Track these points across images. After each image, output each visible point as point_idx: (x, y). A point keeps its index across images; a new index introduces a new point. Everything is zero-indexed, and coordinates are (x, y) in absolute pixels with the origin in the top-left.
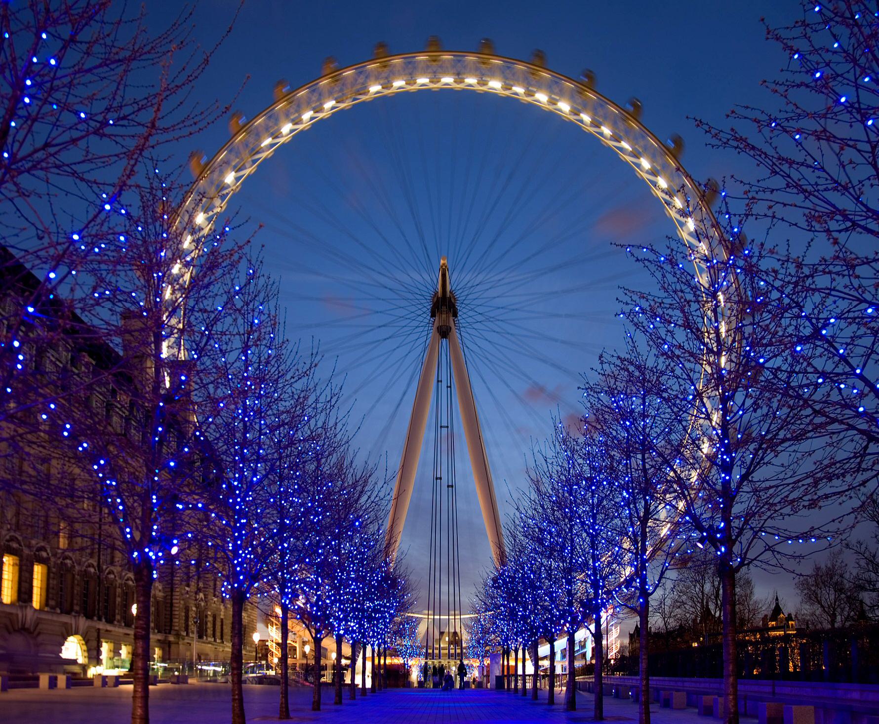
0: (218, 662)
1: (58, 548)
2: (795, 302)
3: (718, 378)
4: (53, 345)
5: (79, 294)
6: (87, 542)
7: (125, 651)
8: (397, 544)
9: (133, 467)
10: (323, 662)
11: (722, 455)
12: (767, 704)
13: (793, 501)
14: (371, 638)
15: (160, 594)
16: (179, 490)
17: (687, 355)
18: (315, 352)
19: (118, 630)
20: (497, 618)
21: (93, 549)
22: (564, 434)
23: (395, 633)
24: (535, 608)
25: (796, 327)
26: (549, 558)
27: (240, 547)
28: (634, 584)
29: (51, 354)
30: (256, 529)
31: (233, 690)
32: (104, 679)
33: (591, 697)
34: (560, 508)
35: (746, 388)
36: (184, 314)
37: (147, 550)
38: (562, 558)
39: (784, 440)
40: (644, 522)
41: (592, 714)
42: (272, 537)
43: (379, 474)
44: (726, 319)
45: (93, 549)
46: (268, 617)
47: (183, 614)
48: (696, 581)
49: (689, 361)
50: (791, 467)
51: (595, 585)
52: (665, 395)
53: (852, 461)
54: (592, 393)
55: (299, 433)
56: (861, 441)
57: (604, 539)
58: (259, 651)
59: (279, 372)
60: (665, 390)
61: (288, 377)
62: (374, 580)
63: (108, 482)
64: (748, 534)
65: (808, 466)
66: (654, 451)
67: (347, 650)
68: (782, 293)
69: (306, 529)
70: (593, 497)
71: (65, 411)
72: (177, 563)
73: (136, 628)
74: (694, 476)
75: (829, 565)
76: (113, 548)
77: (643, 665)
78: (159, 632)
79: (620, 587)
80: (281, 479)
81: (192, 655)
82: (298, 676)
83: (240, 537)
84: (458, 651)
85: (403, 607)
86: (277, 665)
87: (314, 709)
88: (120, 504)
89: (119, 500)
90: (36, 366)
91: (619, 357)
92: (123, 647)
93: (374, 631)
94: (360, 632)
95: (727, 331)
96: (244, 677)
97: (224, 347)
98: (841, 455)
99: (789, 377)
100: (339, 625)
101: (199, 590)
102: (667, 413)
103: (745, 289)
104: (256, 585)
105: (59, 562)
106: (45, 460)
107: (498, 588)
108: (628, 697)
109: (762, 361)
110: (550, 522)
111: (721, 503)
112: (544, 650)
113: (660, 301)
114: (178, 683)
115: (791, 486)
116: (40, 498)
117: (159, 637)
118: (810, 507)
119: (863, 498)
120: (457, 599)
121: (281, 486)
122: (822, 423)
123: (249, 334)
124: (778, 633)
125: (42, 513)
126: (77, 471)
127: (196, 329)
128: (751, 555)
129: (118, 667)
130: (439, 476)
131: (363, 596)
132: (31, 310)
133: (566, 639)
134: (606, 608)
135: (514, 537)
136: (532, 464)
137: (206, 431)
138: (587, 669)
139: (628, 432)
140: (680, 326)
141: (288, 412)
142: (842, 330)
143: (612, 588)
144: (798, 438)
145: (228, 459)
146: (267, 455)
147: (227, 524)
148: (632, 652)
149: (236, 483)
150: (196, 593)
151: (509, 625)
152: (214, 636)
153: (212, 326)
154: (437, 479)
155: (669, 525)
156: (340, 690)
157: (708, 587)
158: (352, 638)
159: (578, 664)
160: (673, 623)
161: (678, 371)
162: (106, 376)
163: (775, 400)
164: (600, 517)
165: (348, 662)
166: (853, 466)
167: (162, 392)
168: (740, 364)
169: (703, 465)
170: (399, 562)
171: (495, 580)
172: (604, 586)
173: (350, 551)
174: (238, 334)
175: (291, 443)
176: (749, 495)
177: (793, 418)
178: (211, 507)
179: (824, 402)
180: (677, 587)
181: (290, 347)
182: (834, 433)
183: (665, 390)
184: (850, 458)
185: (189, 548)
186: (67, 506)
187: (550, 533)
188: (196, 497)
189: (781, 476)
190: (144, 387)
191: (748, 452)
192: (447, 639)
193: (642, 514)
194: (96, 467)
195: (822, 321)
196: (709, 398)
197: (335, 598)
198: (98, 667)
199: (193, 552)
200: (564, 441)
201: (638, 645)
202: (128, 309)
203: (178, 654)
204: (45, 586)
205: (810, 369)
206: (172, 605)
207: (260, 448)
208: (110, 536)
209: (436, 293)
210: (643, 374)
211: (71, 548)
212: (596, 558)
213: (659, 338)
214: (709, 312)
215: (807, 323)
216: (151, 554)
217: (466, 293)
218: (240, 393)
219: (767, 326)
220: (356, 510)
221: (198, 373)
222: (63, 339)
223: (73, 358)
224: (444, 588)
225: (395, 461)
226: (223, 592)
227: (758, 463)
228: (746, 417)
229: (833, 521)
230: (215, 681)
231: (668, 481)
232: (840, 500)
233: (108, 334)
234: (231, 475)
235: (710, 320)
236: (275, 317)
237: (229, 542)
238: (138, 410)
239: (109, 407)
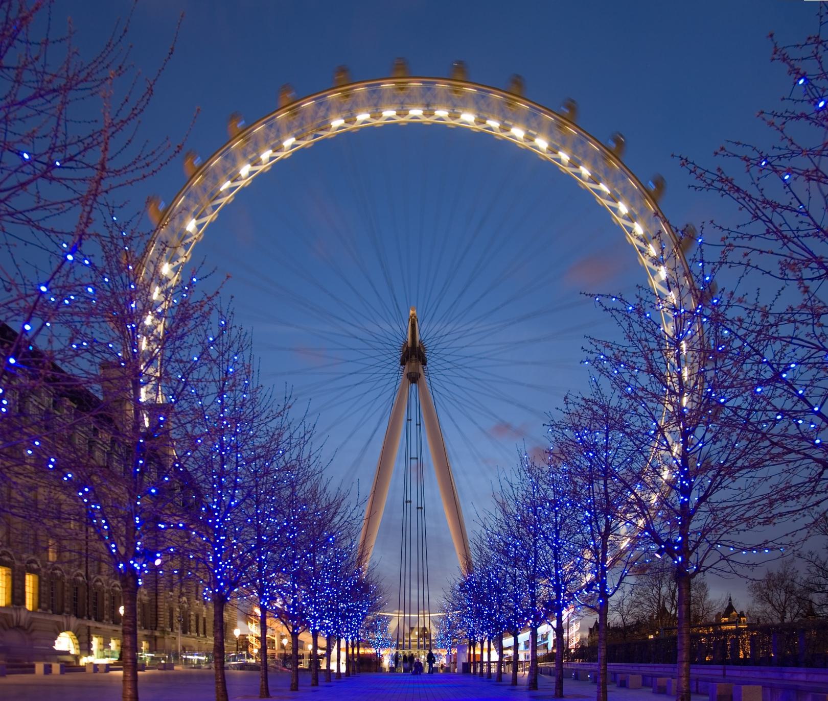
0: (200, 652)
1: (48, 561)
2: (755, 350)
3: (680, 415)
4: (33, 391)
5: (57, 346)
6: (74, 556)
7: (114, 645)
8: (369, 556)
9: (117, 494)
10: (300, 652)
11: (682, 480)
12: (718, 685)
13: (749, 518)
14: (345, 632)
15: (145, 599)
16: (161, 513)
17: (650, 396)
18: (288, 396)
19: (108, 627)
20: (464, 616)
21: (81, 562)
22: (530, 464)
23: (367, 628)
24: (500, 608)
25: (757, 371)
26: (514, 566)
27: (220, 559)
28: (594, 588)
29: (33, 399)
30: (234, 544)
31: (216, 675)
32: (96, 667)
33: (553, 679)
34: (525, 525)
35: (707, 424)
36: (161, 364)
37: (132, 562)
38: (526, 566)
39: (741, 468)
40: (605, 537)
41: (553, 693)
42: (250, 551)
43: (351, 500)
44: (689, 365)
45: (81, 562)
46: (247, 617)
47: (168, 614)
48: (653, 585)
49: (652, 401)
50: (748, 491)
51: (557, 589)
52: (628, 430)
53: (806, 485)
54: (557, 429)
55: (275, 464)
56: (816, 468)
57: (566, 551)
58: (239, 643)
59: (254, 413)
60: (628, 426)
61: (263, 417)
62: (347, 586)
63: (93, 506)
64: (704, 546)
65: (764, 489)
66: (616, 477)
67: (322, 642)
68: (744, 341)
69: (282, 544)
70: (556, 516)
71: (49, 447)
72: (161, 572)
73: (124, 625)
74: (654, 498)
75: (781, 572)
76: (100, 560)
77: (602, 653)
78: (145, 628)
79: (581, 590)
80: (258, 503)
81: (177, 647)
82: (277, 664)
83: (220, 551)
84: (427, 643)
85: (375, 607)
86: (257, 655)
87: (292, 690)
88: (105, 524)
89: (103, 521)
90: (20, 410)
91: (583, 399)
92: (112, 641)
93: (347, 627)
94: (334, 628)
95: (689, 376)
96: (226, 664)
97: (200, 392)
98: (796, 480)
99: (748, 415)
100: (315, 623)
101: (182, 595)
102: (629, 445)
103: (709, 338)
104: (236, 590)
105: (49, 572)
106: (32, 488)
107: (466, 591)
108: (587, 679)
109: (722, 400)
110: (515, 537)
111: (680, 521)
112: (508, 641)
113: (624, 349)
114: (164, 669)
115: (747, 506)
116: (29, 519)
117: (146, 632)
118: (764, 523)
119: (816, 516)
120: (426, 600)
121: (257, 509)
122: (779, 453)
123: (224, 381)
124: (730, 627)
125: (32, 532)
126: (63, 497)
127: (173, 377)
128: (706, 564)
129: (108, 657)
130: (409, 499)
131: (337, 599)
132: (12, 361)
133: (529, 632)
134: (567, 607)
135: (481, 550)
136: (497, 488)
137: (184, 463)
138: (549, 657)
139: (591, 462)
140: (643, 371)
141: (263, 447)
142: (802, 374)
143: (573, 591)
144: (755, 466)
145: (207, 486)
146: (244, 483)
147: (207, 540)
148: (592, 643)
149: (214, 507)
150: (179, 597)
151: (475, 622)
152: (197, 631)
153: (188, 374)
154: (407, 502)
155: (629, 539)
156: (317, 674)
157: (664, 590)
158: (327, 633)
159: (540, 653)
160: (630, 620)
161: (641, 410)
162: (87, 417)
163: (734, 434)
164: (563, 533)
165: (324, 652)
166: (807, 489)
167: (142, 431)
168: (701, 404)
169: (663, 489)
170: (371, 570)
171: (462, 586)
172: (566, 590)
173: (325, 562)
174: (214, 380)
175: (267, 473)
176: (706, 514)
177: (751, 449)
178: (192, 526)
179: (781, 436)
180: (635, 590)
181: (264, 392)
182: (790, 462)
183: (628, 426)
184: (805, 483)
185: (172, 560)
186: (55, 526)
187: (515, 546)
188: (177, 518)
189: (738, 498)
190: (125, 426)
191: (707, 478)
192: (417, 633)
193: (603, 530)
194: (80, 494)
195: (783, 366)
196: (670, 432)
197: (311, 600)
198: (89, 657)
199: (176, 563)
200: (529, 470)
201: (597, 637)
202: (107, 360)
203: (164, 646)
204: (36, 591)
205: (769, 408)
206: (157, 607)
207: (237, 477)
208: (96, 551)
209: (406, 343)
210: (607, 412)
211: (60, 560)
212: (558, 567)
213: (623, 382)
214: (672, 360)
215: (768, 368)
216: (136, 565)
217: (435, 343)
218: (217, 431)
219: (729, 371)
220: (330, 528)
221: (176, 414)
222: (45, 386)
223: (55, 402)
224: (414, 592)
225: (367, 487)
226: (205, 596)
227: (716, 487)
228: (706, 449)
229: (787, 535)
230: (200, 668)
231: (628, 503)
232: (794, 518)
233: (88, 382)
234: (210, 500)
235: (674, 366)
236: (249, 366)
237: (209, 556)
238: (119, 446)
239: (91, 444)
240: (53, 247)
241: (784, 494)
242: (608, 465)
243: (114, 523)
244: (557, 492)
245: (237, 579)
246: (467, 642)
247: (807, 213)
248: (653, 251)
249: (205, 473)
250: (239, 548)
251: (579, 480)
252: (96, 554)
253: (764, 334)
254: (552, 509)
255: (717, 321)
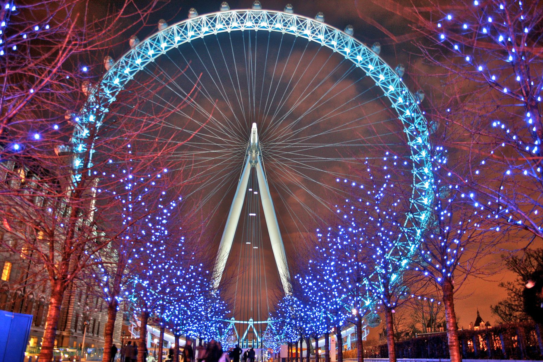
47: (75, 319)
101: (87, 304)
150: (84, 306)
152: (93, 332)
206: (68, 313)
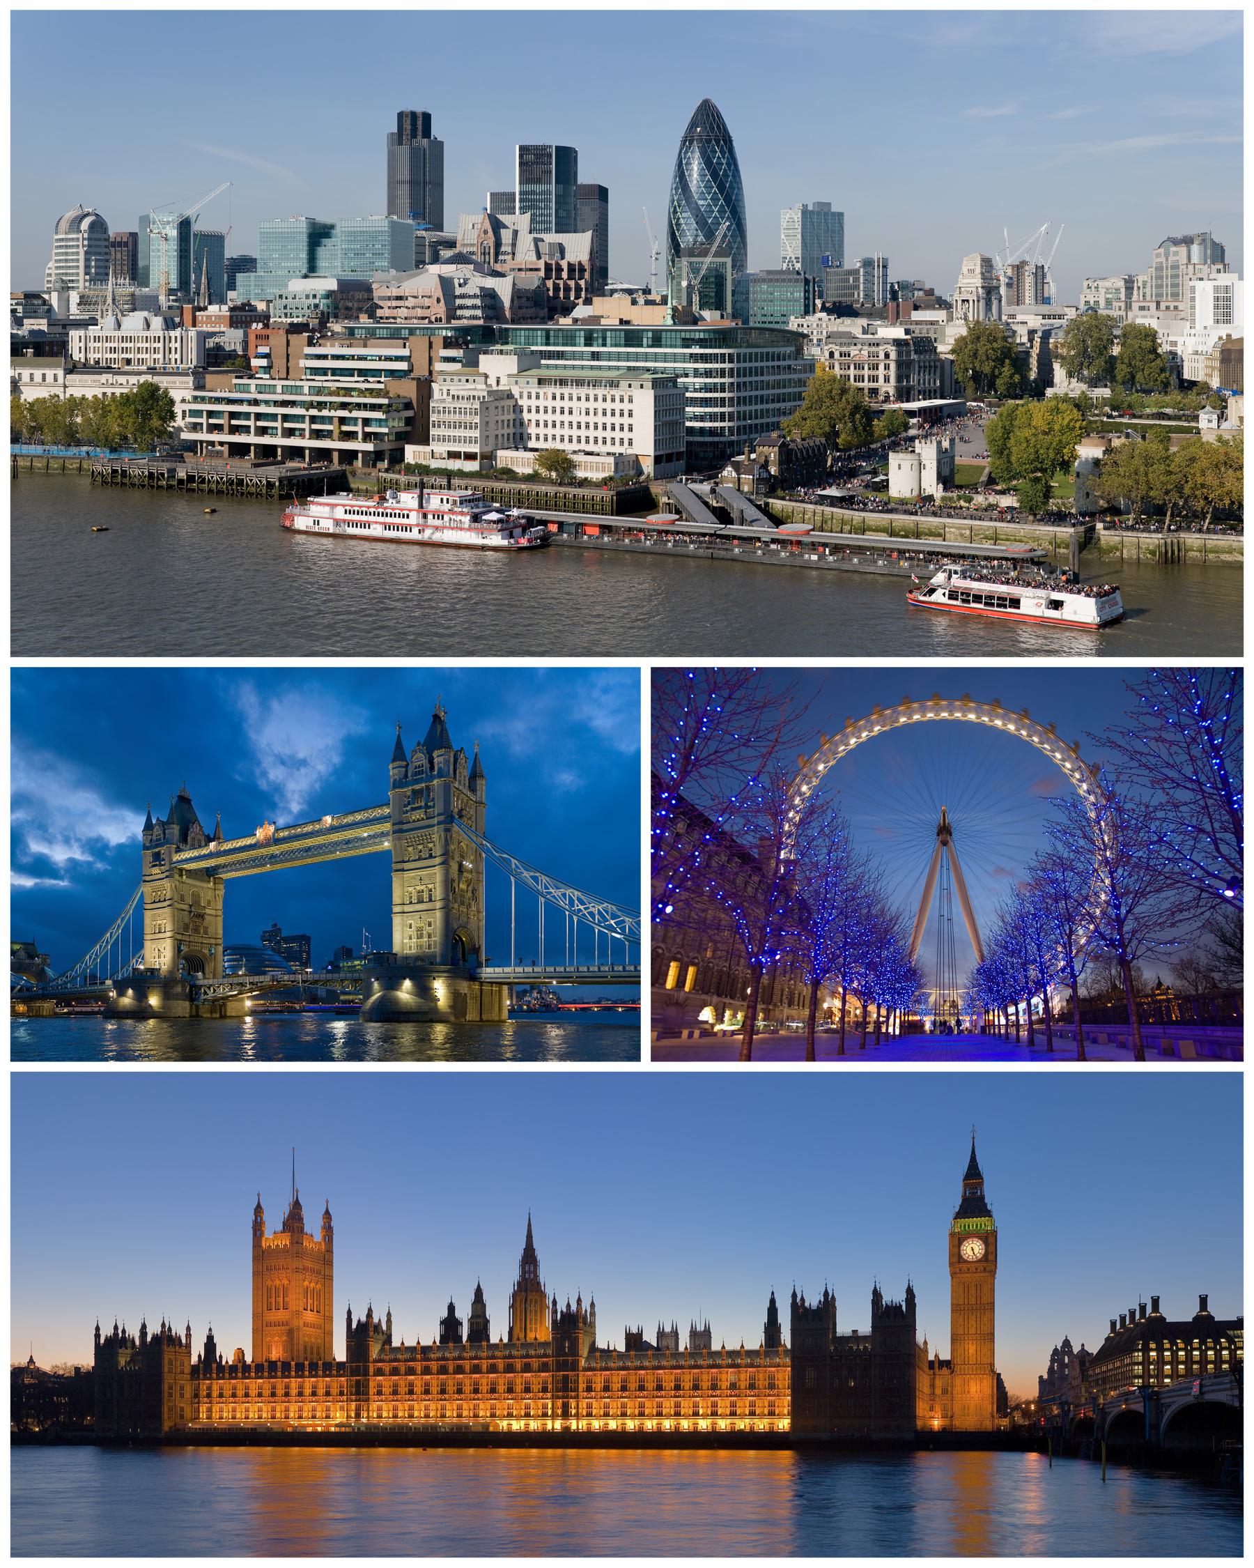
3: (1106, 862)
6: (724, 953)
34: (1017, 930)
39: (1150, 892)
42: (839, 949)
43: (906, 914)
46: (833, 994)
51: (1042, 972)
64: (1135, 942)
65: (1166, 905)
67: (883, 1012)
74: (1098, 912)
76: (740, 957)
77: (1077, 1018)
80: (846, 918)
83: (819, 949)
85: (920, 986)
98: (1185, 899)
101: (791, 979)
102: (1078, 879)
106: (705, 911)
112: (1011, 1010)
118: (1171, 926)
126: (723, 916)
128: (1138, 953)
138: (1040, 1021)
144: (1159, 890)
148: (1069, 1010)
157: (1113, 972)
159: (1034, 1018)
160: (1093, 993)
161: (1082, 859)
164: (1042, 934)
170: (918, 961)
199: (789, 958)
200: (1018, 895)
211: (713, 957)
212: (1041, 957)
224: (946, 975)
228: (1125, 881)
240: (743, 779)
241: (1180, 908)
242: (1066, 892)
243: (753, 932)
244: (1036, 909)
245: (829, 968)
246: (983, 1010)
247: (1159, 757)
248: (1077, 776)
249: (814, 900)
250: (832, 947)
251: (1050, 901)
252: (737, 953)
253: (1148, 817)
254: (1033, 920)
255: (1120, 810)
